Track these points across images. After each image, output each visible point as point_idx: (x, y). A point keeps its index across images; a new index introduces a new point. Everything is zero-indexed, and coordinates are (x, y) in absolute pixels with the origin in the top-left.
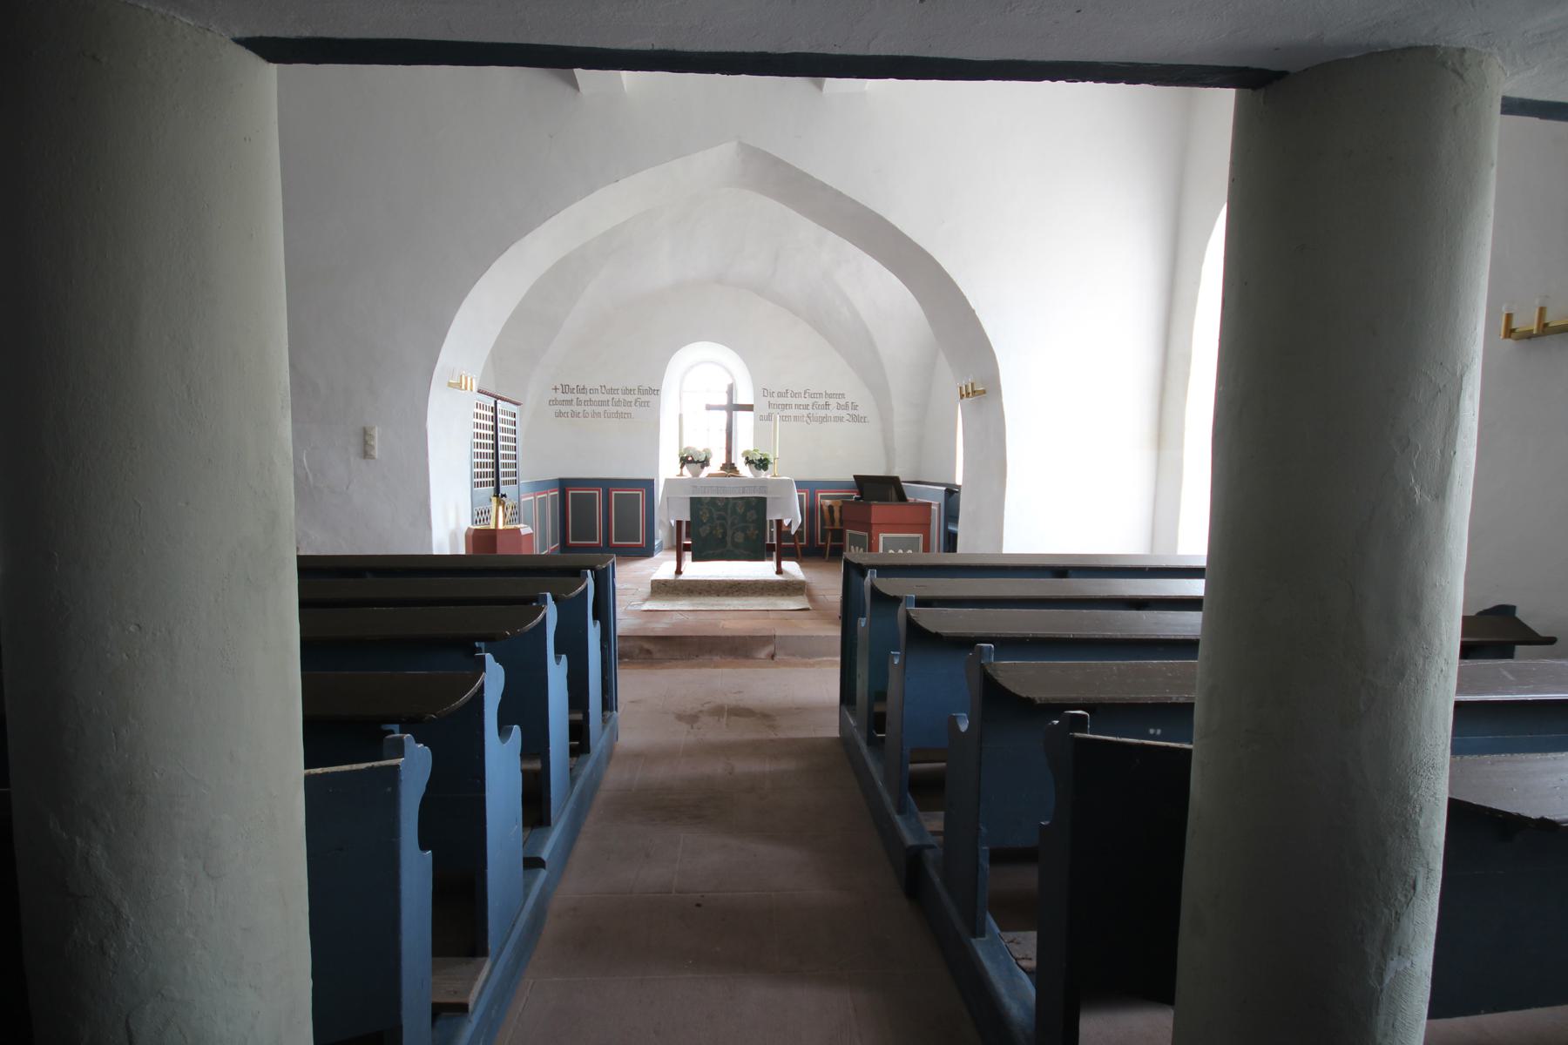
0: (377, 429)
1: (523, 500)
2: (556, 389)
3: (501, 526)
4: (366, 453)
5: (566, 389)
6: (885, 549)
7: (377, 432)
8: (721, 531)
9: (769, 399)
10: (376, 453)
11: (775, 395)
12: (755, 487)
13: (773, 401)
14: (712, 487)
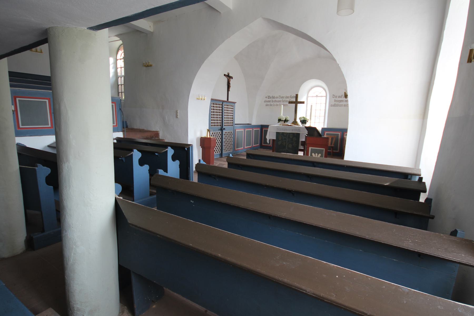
0: (179, 111)
1: (237, 130)
2: (266, 97)
3: (208, 137)
4: (177, 117)
5: (269, 97)
6: (311, 155)
7: (178, 112)
8: (285, 143)
9: (335, 98)
10: (178, 117)
11: (337, 97)
12: (296, 129)
13: (336, 99)
14: (283, 129)
